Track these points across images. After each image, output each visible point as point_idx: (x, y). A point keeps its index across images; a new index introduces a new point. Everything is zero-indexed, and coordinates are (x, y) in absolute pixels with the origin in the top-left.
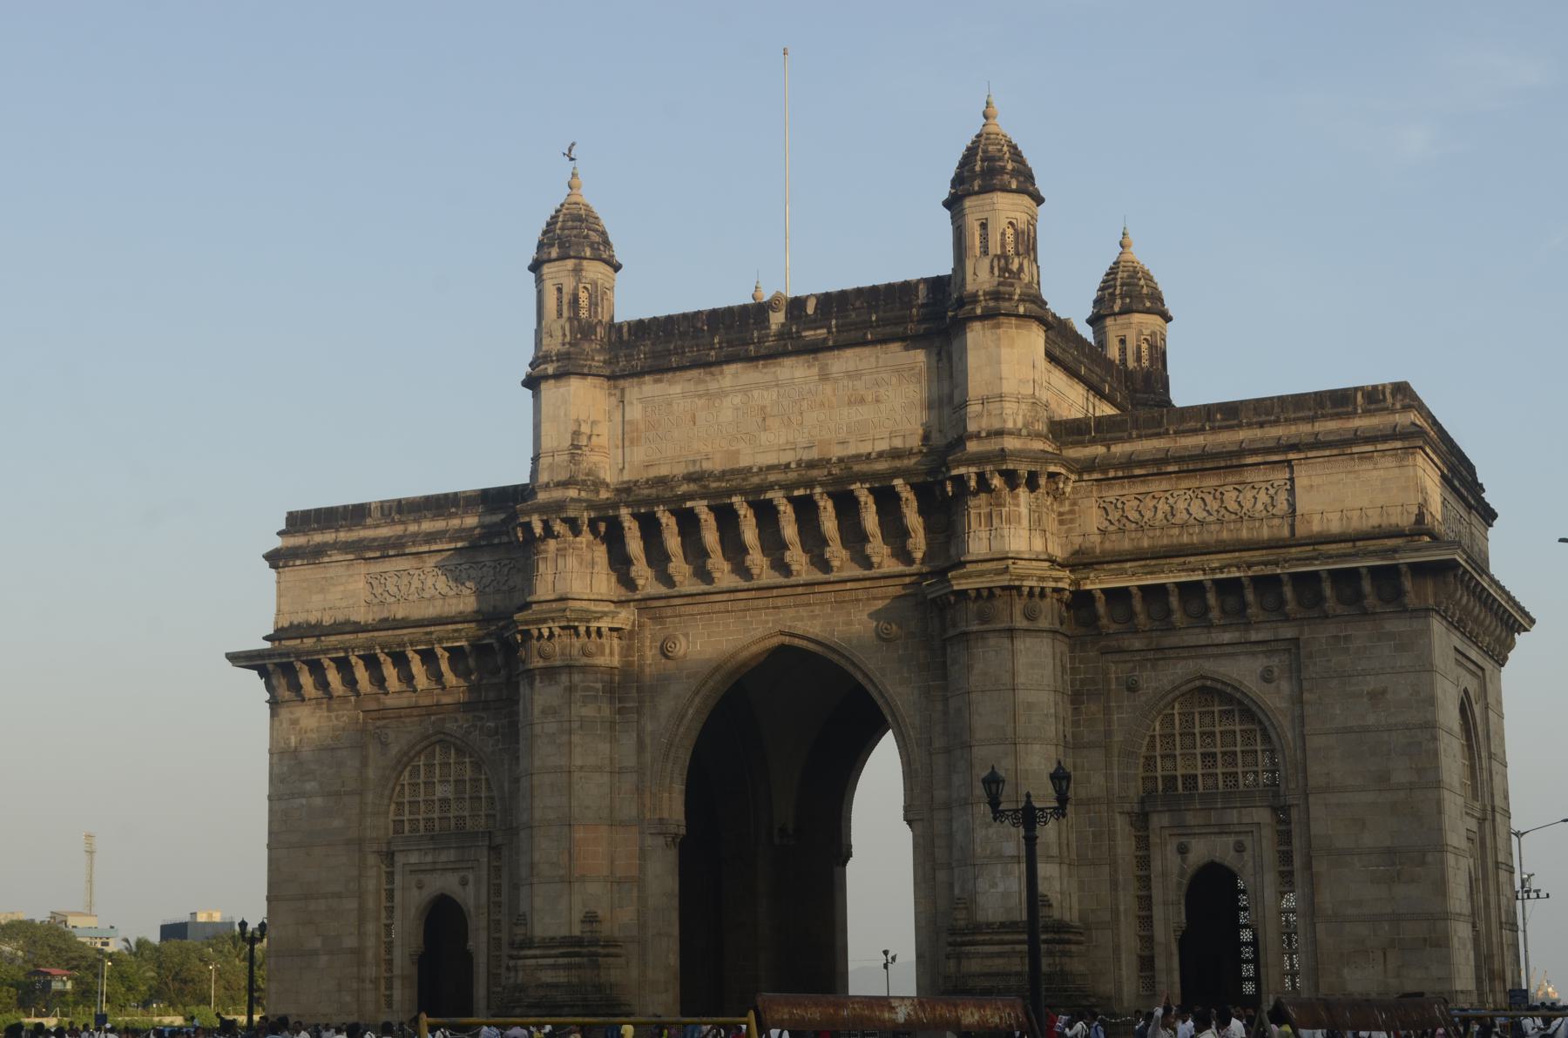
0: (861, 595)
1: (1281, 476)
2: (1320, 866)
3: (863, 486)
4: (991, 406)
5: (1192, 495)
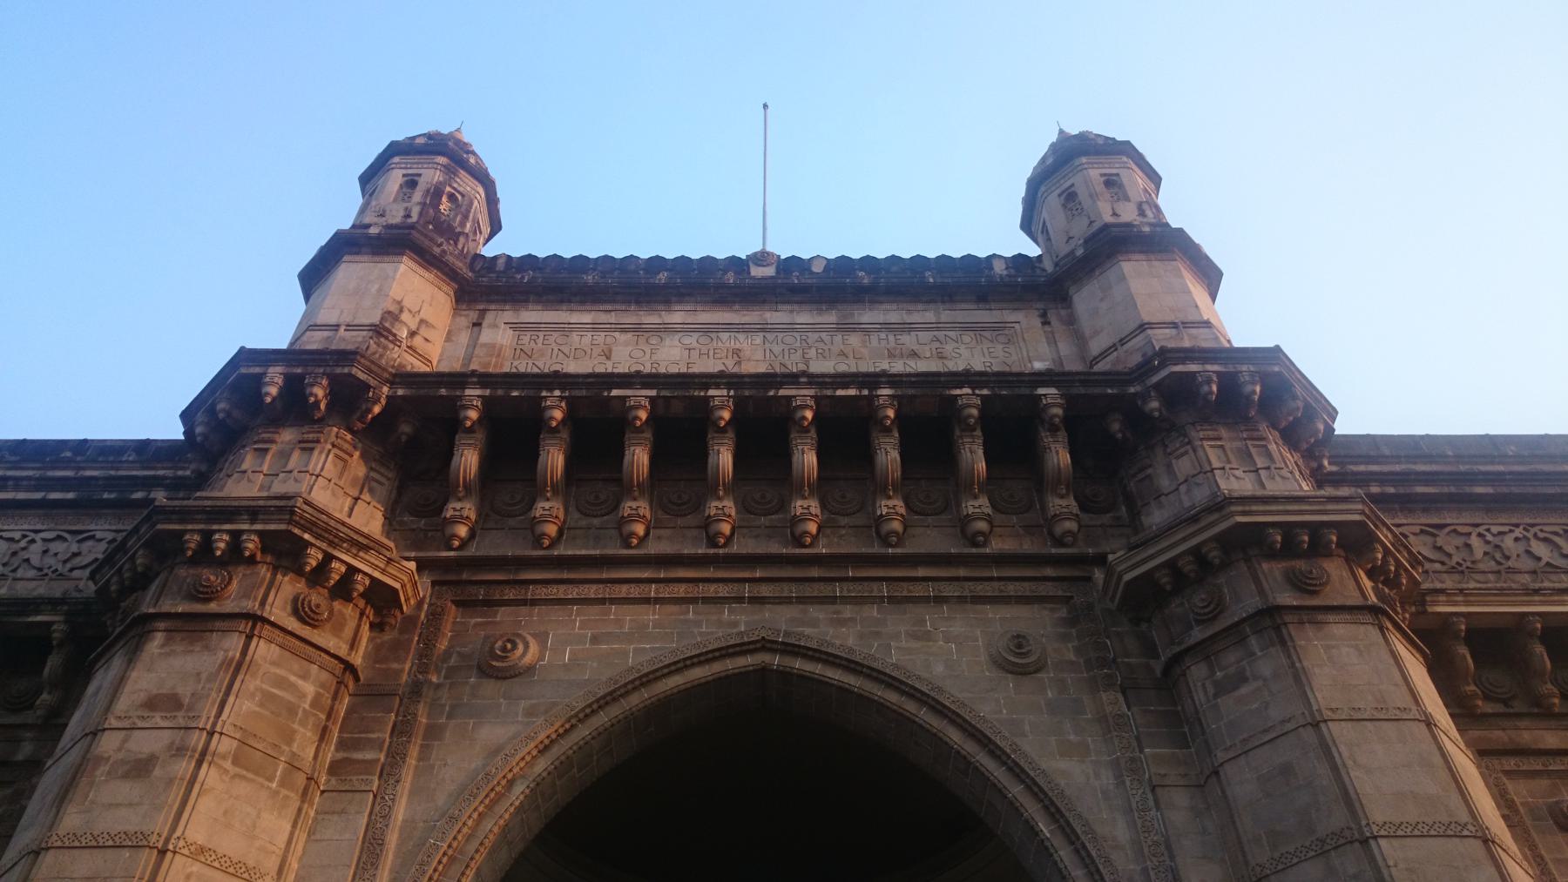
0: (949, 590)
3: (977, 392)
4: (1194, 331)
5: (1529, 535)
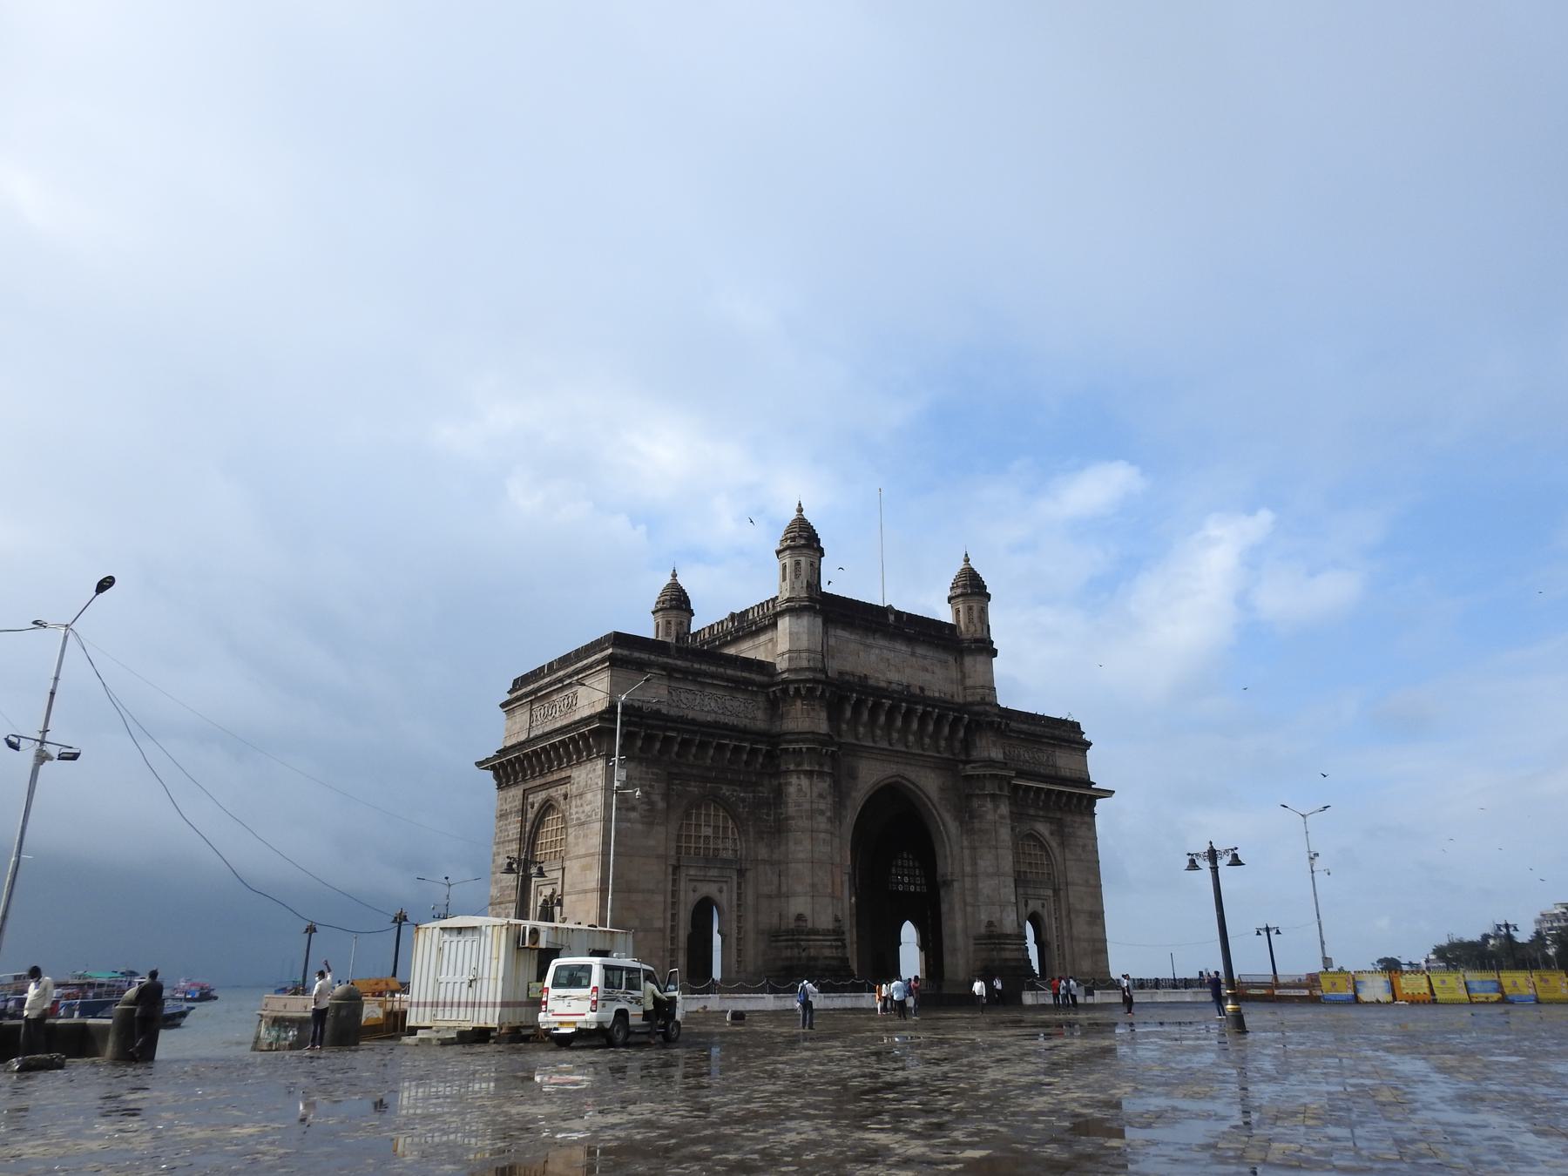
1: (1050, 750)
2: (1073, 916)
